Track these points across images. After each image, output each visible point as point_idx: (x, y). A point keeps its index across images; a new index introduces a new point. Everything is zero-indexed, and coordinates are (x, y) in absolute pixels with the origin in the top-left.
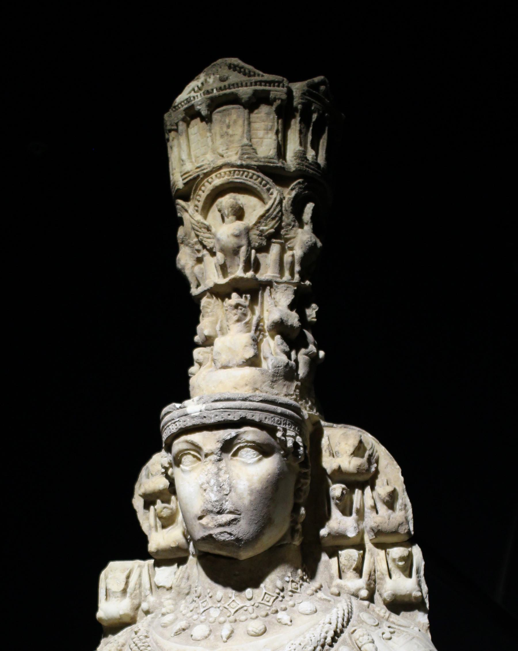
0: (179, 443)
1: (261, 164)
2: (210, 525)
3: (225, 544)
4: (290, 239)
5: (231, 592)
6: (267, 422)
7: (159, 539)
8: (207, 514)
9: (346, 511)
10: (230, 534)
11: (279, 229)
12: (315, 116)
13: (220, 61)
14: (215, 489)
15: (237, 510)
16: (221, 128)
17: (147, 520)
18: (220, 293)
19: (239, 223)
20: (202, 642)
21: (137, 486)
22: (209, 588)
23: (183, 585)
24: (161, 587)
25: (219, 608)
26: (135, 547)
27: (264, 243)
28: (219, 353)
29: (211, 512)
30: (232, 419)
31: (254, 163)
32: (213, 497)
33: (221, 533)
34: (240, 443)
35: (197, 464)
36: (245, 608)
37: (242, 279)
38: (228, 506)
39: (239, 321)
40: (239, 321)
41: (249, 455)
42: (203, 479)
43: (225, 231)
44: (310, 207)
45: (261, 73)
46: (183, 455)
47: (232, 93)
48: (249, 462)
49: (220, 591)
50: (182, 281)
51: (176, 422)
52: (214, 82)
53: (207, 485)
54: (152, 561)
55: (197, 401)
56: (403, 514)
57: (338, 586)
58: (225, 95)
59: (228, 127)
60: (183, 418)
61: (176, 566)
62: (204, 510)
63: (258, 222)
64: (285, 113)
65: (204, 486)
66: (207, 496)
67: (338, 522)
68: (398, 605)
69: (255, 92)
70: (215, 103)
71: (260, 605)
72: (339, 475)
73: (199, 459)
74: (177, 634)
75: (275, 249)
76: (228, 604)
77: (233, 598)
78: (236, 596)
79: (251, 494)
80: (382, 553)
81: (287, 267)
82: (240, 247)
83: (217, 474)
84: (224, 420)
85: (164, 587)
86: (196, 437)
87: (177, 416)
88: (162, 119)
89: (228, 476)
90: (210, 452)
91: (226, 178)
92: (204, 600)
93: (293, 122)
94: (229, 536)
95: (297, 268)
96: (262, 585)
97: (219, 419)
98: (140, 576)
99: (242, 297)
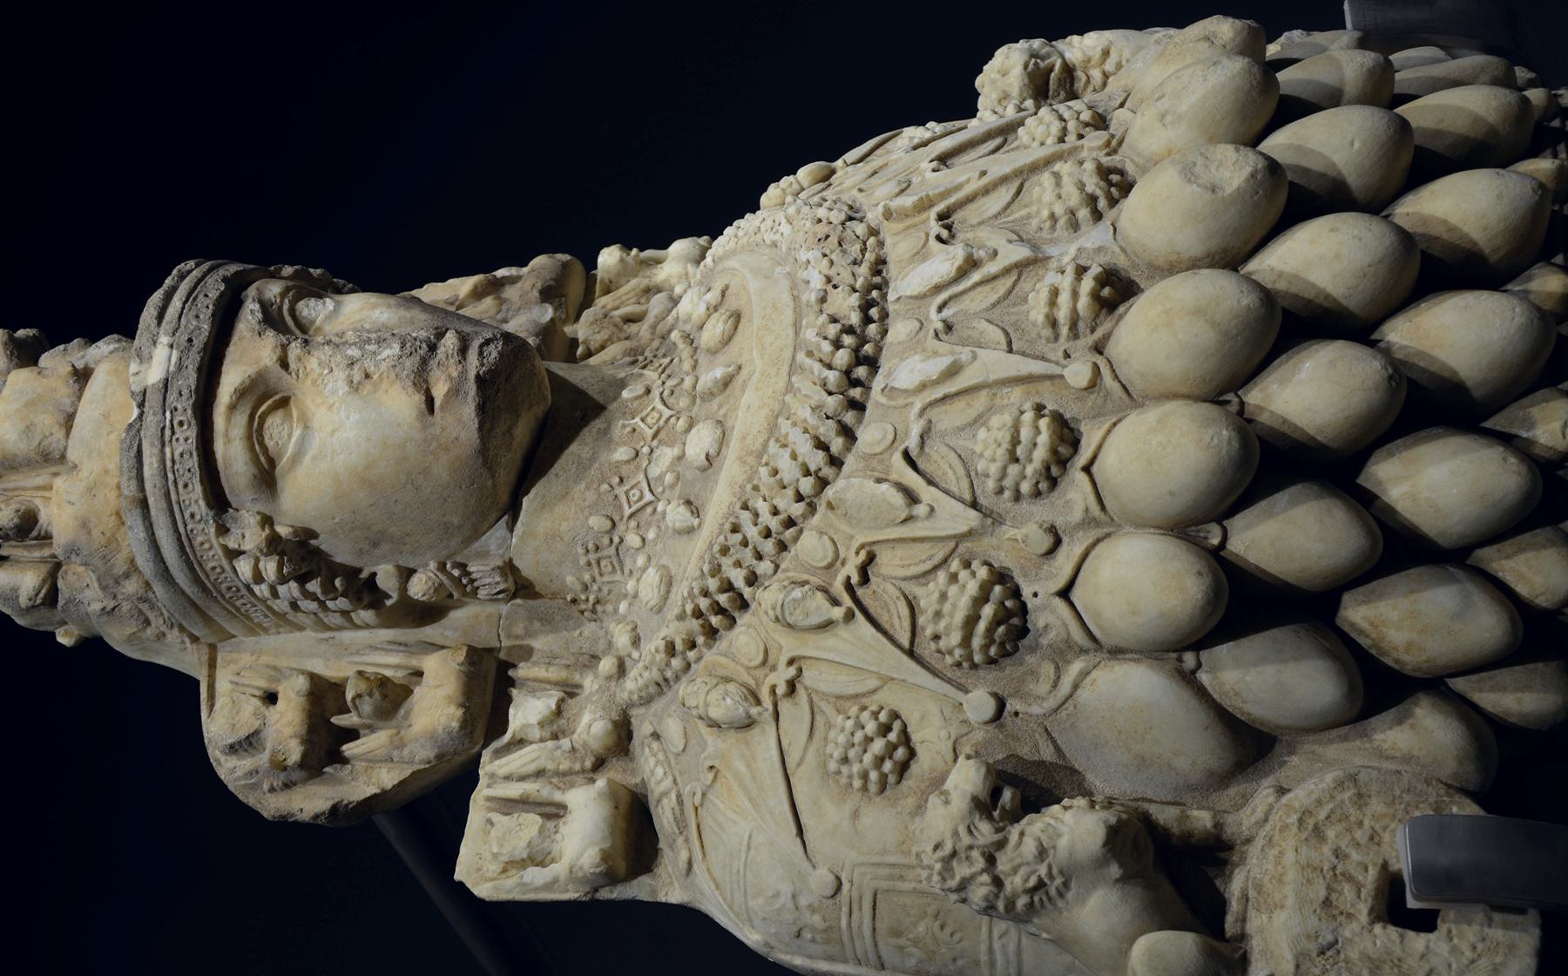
0: (226, 434)
2: (455, 374)
8: (426, 381)
10: (487, 342)
14: (372, 348)
17: (376, 767)
20: (729, 424)
21: (271, 805)
22: (597, 489)
29: (424, 362)
33: (481, 353)
34: (280, 308)
36: (666, 393)
42: (338, 382)
53: (356, 367)
60: (172, 397)
61: (514, 692)
65: (357, 375)
66: (383, 366)
71: (668, 371)
73: (284, 403)
80: (602, 302)
85: (560, 703)
86: (231, 379)
87: (159, 417)
90: (279, 350)
92: (623, 499)
94: (492, 346)
97: (206, 315)
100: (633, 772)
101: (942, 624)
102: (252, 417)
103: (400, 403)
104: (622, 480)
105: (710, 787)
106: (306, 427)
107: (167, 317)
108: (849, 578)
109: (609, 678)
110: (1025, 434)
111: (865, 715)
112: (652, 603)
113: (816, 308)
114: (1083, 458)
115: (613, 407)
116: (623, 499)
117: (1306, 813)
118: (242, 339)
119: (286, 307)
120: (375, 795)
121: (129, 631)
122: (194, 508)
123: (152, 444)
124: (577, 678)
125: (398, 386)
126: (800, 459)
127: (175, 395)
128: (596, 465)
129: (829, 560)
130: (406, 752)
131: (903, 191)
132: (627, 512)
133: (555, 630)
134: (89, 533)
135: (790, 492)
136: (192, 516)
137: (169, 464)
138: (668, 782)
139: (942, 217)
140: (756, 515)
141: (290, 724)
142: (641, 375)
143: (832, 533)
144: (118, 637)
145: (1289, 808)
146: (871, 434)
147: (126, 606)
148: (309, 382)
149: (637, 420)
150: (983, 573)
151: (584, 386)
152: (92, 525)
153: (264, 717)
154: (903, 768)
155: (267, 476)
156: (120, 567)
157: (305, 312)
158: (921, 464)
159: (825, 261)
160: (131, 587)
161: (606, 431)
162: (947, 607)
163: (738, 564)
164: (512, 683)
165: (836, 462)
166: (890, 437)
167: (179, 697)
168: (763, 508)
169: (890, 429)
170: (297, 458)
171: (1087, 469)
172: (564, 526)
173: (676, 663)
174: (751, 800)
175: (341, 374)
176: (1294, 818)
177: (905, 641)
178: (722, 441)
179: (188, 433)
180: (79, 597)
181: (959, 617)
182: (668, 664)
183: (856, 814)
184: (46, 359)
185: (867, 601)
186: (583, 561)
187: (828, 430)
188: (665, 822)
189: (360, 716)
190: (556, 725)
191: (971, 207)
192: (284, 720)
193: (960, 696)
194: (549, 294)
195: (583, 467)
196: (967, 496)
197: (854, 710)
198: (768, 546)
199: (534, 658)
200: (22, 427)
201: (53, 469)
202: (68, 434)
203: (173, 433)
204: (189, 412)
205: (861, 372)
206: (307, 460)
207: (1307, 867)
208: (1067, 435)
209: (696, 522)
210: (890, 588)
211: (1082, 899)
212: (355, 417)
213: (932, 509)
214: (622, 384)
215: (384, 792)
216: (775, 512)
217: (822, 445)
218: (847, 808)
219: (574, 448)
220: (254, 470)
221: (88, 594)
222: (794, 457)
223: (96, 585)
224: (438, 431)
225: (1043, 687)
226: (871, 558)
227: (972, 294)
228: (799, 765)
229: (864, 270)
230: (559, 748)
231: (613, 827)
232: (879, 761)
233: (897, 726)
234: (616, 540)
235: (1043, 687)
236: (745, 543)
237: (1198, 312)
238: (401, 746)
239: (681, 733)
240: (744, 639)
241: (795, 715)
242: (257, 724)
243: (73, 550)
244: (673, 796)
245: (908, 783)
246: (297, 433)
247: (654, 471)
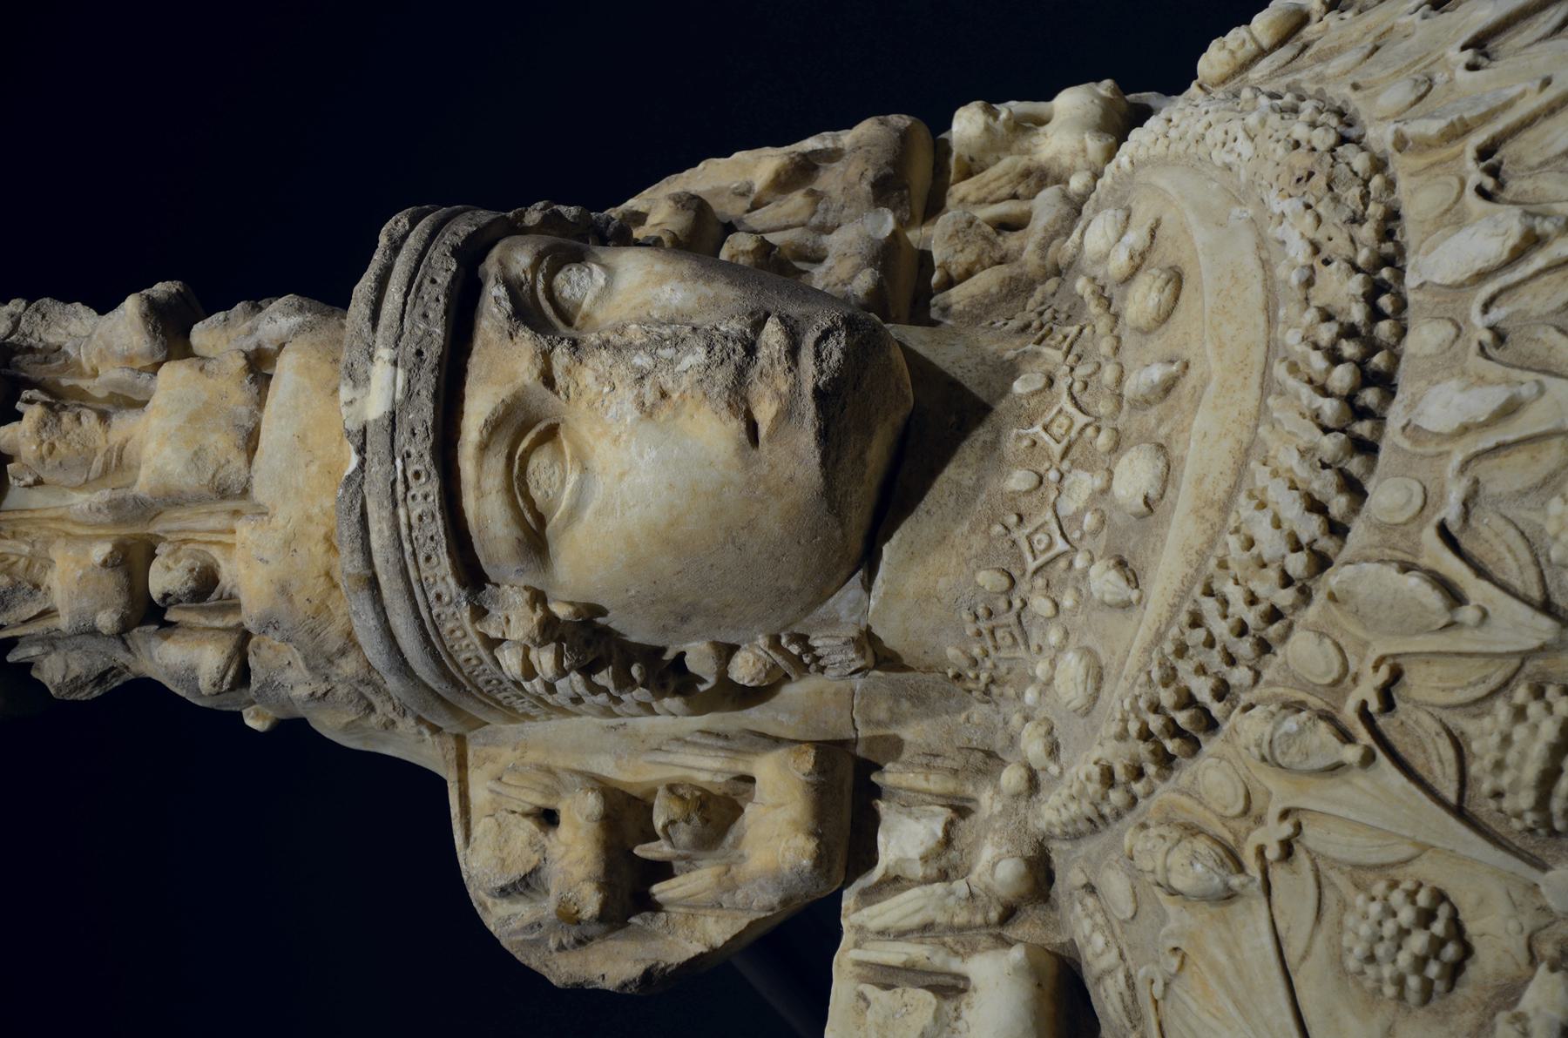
2: (784, 388)
8: (745, 400)
10: (825, 335)
14: (667, 353)
15: (752, 314)
17: (701, 915)
20: (1176, 451)
21: (563, 969)
22: (987, 532)
24: (947, 832)
25: (1062, 476)
28: (198, 455)
29: (741, 372)
30: (449, 276)
32: (696, 357)
33: (818, 354)
34: (533, 289)
35: (565, 443)
36: (1077, 386)
39: (104, 417)
40: (104, 417)
48: (602, 282)
51: (404, 471)
53: (648, 382)
55: (355, 386)
60: (402, 437)
61: (882, 806)
62: (730, 405)
65: (650, 396)
66: (686, 381)
71: (1076, 350)
73: (551, 434)
74: (1133, 580)
76: (1052, 443)
77: (1038, 428)
78: (1032, 425)
79: (709, 281)
80: (961, 190)
83: (618, 349)
84: (446, 296)
85: (949, 826)
86: (478, 407)
87: (388, 466)
89: (634, 326)
90: (539, 361)
92: (1025, 547)
94: (832, 341)
97: (437, 312)
99: (19, 416)
100: (1058, 926)
101: (1505, 780)
102: (510, 458)
103: (710, 432)
104: (1021, 518)
105: (1176, 975)
106: (584, 469)
107: (384, 320)
108: (1364, 704)
109: (1016, 796)
111: (1397, 897)
112: (1075, 704)
113: (1299, 295)
115: (1001, 406)
116: (1025, 547)
118: (486, 344)
119: (540, 286)
120: (702, 954)
121: (346, 719)
122: (441, 587)
123: (381, 505)
124: (969, 790)
125: (707, 408)
126: (1286, 526)
127: (407, 435)
128: (983, 497)
129: (1335, 675)
130: (740, 895)
131: (1420, 98)
132: (1032, 565)
133: (931, 713)
134: (290, 600)
135: (1272, 574)
136: (439, 597)
137: (404, 531)
138: (1111, 958)
139: (1484, 153)
140: (1225, 603)
141: (581, 861)
142: (1038, 354)
143: (1336, 634)
144: (331, 724)
146: (1388, 495)
147: (341, 690)
148: (583, 405)
149: (1038, 428)
151: (956, 372)
152: (293, 591)
153: (544, 849)
154: (1455, 972)
155: (535, 539)
156: (334, 642)
157: (567, 292)
158: (1465, 542)
159: (1309, 219)
160: (348, 667)
161: (994, 446)
162: (1512, 756)
163: (1201, 670)
164: (877, 792)
165: (1337, 530)
166: (1417, 501)
167: (415, 809)
168: (1235, 594)
169: (1417, 489)
170: (574, 513)
172: (943, 583)
173: (1117, 797)
174: (1236, 1002)
175: (627, 394)
177: (1450, 793)
178: (1167, 477)
179: (428, 488)
180: (278, 679)
181: (1531, 772)
182: (1105, 797)
184: (203, 335)
185: (1393, 735)
186: (970, 630)
187: (1324, 485)
188: (1110, 1009)
189: (673, 845)
190: (945, 861)
191: (1529, 135)
192: (573, 856)
193: (1534, 875)
194: (886, 189)
195: (966, 499)
196: (1535, 593)
197: (1380, 888)
198: (1244, 648)
199: (905, 756)
200: (188, 453)
201: (231, 505)
202: (250, 462)
203: (407, 488)
204: (427, 458)
205: (1370, 396)
206: (588, 514)
209: (1134, 595)
210: (1426, 720)
212: (651, 454)
213: (1485, 615)
214: (1011, 370)
215: (714, 951)
216: (1253, 600)
217: (1315, 506)
219: (950, 471)
220: (516, 532)
221: (290, 675)
222: (1277, 524)
223: (301, 664)
224: (765, 469)
226: (1396, 675)
227: (1534, 285)
228: (1303, 958)
229: (1367, 232)
230: (951, 893)
231: (1036, 1014)
232: (1420, 963)
233: (1443, 911)
234: (1017, 604)
236: (1210, 643)
238: (733, 888)
239: (1129, 893)
240: (1213, 776)
241: (1293, 887)
242: (535, 858)
243: (270, 623)
244: (1121, 976)
245: (1464, 992)
246: (573, 478)
247: (1068, 507)
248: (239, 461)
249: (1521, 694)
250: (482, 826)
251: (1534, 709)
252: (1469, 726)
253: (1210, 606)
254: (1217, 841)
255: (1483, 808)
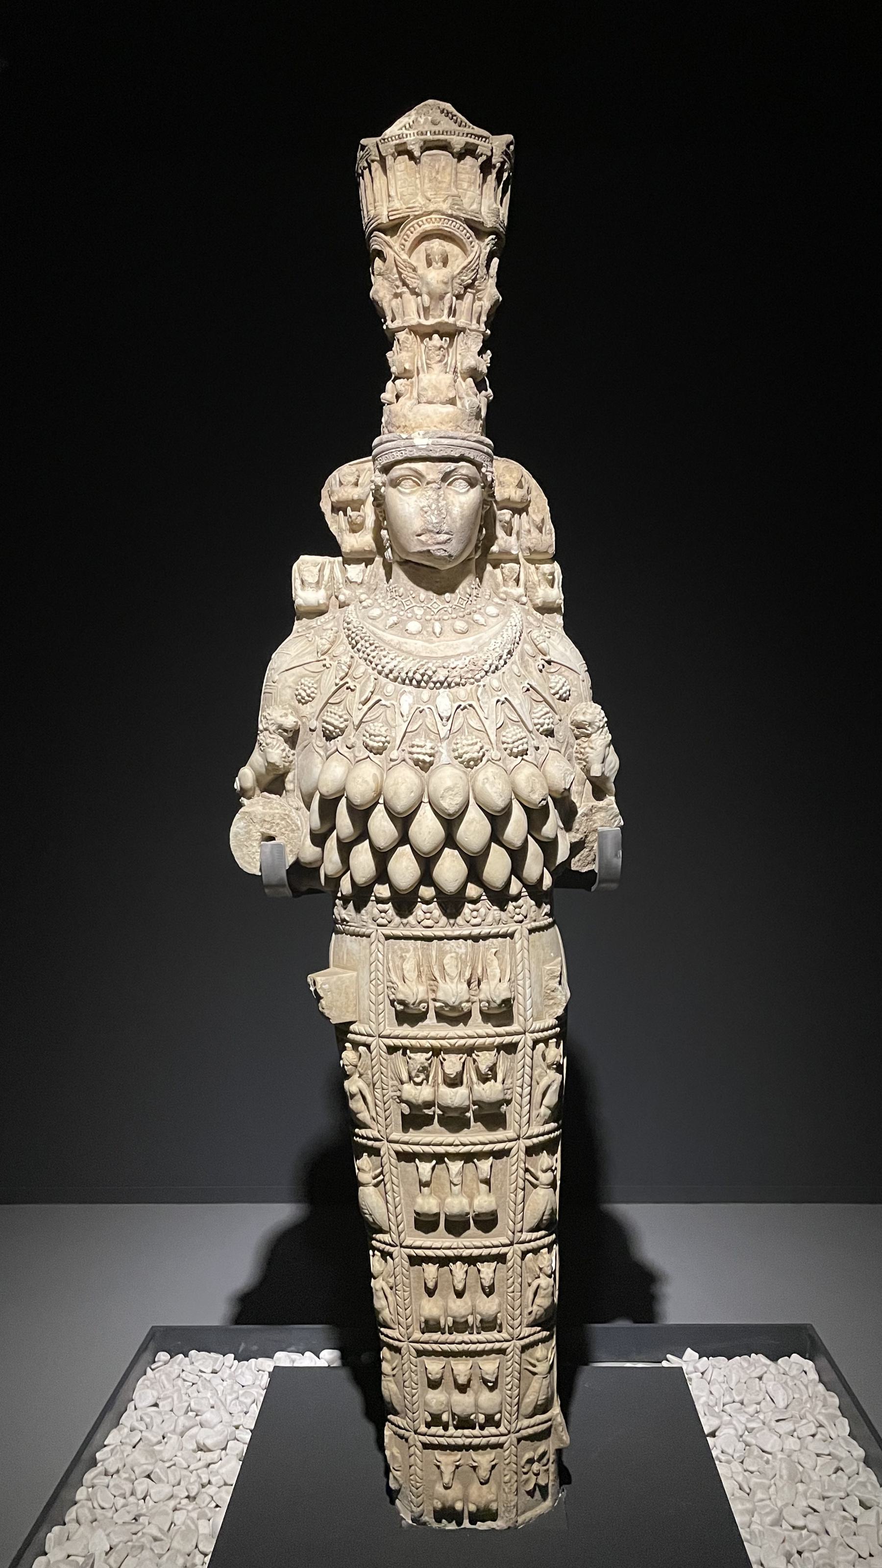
1: (469, 217)
3: (440, 558)
4: (480, 290)
5: (431, 594)
6: (478, 459)
7: (349, 542)
9: (509, 532)
11: (474, 280)
12: (506, 175)
13: (430, 101)
14: (436, 512)
16: (431, 172)
17: (336, 524)
18: (423, 333)
19: (444, 270)
20: (418, 636)
21: (324, 492)
23: (371, 582)
26: (328, 546)
27: (462, 292)
29: (432, 531)
31: (462, 215)
37: (447, 323)
38: (445, 528)
39: (440, 361)
40: (440, 361)
41: (461, 486)
42: (424, 503)
43: (435, 276)
44: (496, 261)
45: (468, 123)
46: (403, 480)
47: (446, 140)
49: (423, 594)
50: (375, 313)
52: (425, 123)
54: (340, 559)
56: (548, 539)
57: (505, 593)
58: (438, 140)
59: (438, 172)
60: (410, 448)
63: (461, 272)
64: (486, 168)
67: (503, 541)
68: (545, 609)
69: (467, 143)
70: (427, 147)
72: (507, 504)
73: (419, 485)
74: (390, 627)
75: (469, 297)
79: (461, 519)
80: (533, 567)
81: (475, 316)
82: (446, 294)
88: (355, 146)
91: (436, 224)
93: (489, 178)
95: (484, 318)
96: (457, 591)
98: (332, 571)
103: (417, 524)
110: (377, 739)
111: (312, 689)
114: (371, 755)
117: (289, 816)
135: (378, 662)
138: (319, 623)
139: (471, 705)
145: (290, 811)
146: (391, 687)
150: (342, 726)
154: (299, 701)
159: (461, 666)
162: (333, 715)
165: (387, 676)
167: (364, 450)
170: (400, 492)
171: (368, 757)
176: (287, 812)
183: (290, 687)
187: (395, 673)
190: (348, 581)
197: (315, 686)
200: (426, 387)
205: (414, 682)
207: (273, 816)
208: (379, 752)
211: (260, 755)
212: (412, 510)
217: (391, 671)
218: (292, 684)
225: (318, 743)
226: (352, 690)
229: (457, 680)
235: (318, 743)
237: (395, 793)
241: (317, 667)
246: (407, 491)
248: (425, 400)
249: (345, 717)
250: (354, 468)
251: (342, 720)
252: (342, 706)
253: (373, 647)
254: (329, 649)
255: (329, 708)
